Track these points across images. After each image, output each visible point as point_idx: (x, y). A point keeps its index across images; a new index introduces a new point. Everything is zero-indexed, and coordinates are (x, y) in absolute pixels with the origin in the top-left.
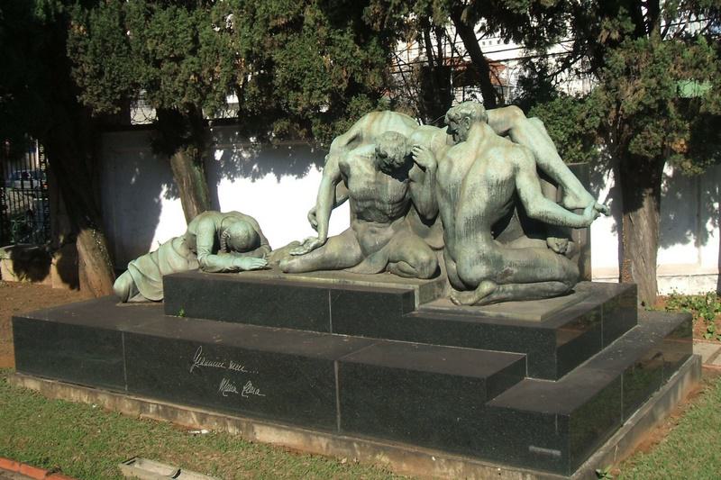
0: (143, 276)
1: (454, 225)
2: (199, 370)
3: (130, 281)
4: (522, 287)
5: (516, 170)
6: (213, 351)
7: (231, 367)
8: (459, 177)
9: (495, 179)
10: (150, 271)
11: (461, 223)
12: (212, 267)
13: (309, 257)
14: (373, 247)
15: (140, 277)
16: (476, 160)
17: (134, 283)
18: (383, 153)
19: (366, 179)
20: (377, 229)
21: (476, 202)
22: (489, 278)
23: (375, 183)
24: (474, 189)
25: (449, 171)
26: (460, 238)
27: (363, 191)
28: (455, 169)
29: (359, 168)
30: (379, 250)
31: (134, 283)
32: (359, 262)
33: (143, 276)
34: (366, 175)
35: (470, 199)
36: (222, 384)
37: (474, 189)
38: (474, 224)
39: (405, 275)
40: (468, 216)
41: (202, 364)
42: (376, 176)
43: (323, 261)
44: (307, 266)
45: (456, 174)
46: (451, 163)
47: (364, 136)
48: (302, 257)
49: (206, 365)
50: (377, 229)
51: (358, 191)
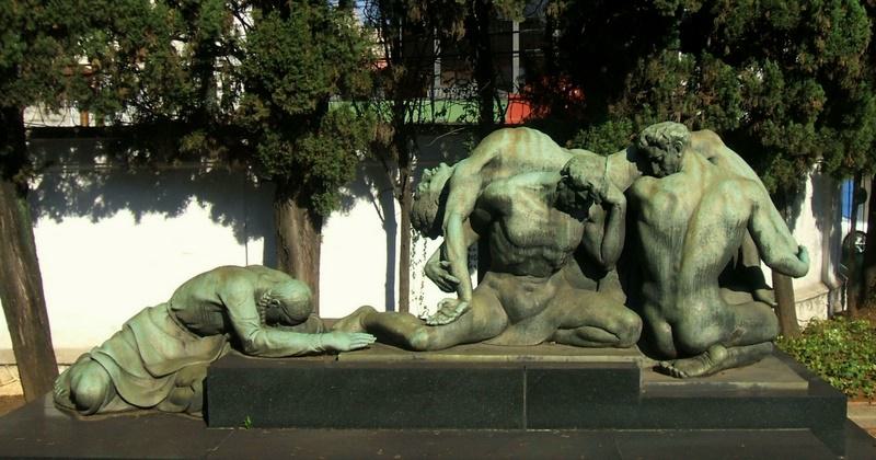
0: (121, 369)
1: (675, 278)
3: (106, 380)
4: (745, 350)
5: (754, 208)
8: (685, 217)
9: (736, 219)
10: (129, 361)
11: (690, 273)
12: (284, 349)
13: (453, 326)
14: (532, 310)
15: (118, 371)
16: (703, 194)
17: (111, 381)
19: (538, 218)
20: (533, 285)
21: (710, 249)
22: (721, 342)
23: (548, 224)
24: (708, 232)
25: (672, 209)
26: (686, 294)
27: (532, 235)
28: (680, 207)
29: (526, 204)
30: (539, 313)
31: (111, 381)
32: (505, 328)
33: (121, 369)
34: (537, 213)
35: (704, 243)
37: (708, 232)
38: (702, 278)
39: (593, 344)
40: (700, 265)
42: (550, 215)
43: (472, 331)
44: (451, 340)
45: (681, 213)
46: (673, 198)
47: (505, 159)
48: (447, 328)
50: (533, 285)
51: (526, 233)
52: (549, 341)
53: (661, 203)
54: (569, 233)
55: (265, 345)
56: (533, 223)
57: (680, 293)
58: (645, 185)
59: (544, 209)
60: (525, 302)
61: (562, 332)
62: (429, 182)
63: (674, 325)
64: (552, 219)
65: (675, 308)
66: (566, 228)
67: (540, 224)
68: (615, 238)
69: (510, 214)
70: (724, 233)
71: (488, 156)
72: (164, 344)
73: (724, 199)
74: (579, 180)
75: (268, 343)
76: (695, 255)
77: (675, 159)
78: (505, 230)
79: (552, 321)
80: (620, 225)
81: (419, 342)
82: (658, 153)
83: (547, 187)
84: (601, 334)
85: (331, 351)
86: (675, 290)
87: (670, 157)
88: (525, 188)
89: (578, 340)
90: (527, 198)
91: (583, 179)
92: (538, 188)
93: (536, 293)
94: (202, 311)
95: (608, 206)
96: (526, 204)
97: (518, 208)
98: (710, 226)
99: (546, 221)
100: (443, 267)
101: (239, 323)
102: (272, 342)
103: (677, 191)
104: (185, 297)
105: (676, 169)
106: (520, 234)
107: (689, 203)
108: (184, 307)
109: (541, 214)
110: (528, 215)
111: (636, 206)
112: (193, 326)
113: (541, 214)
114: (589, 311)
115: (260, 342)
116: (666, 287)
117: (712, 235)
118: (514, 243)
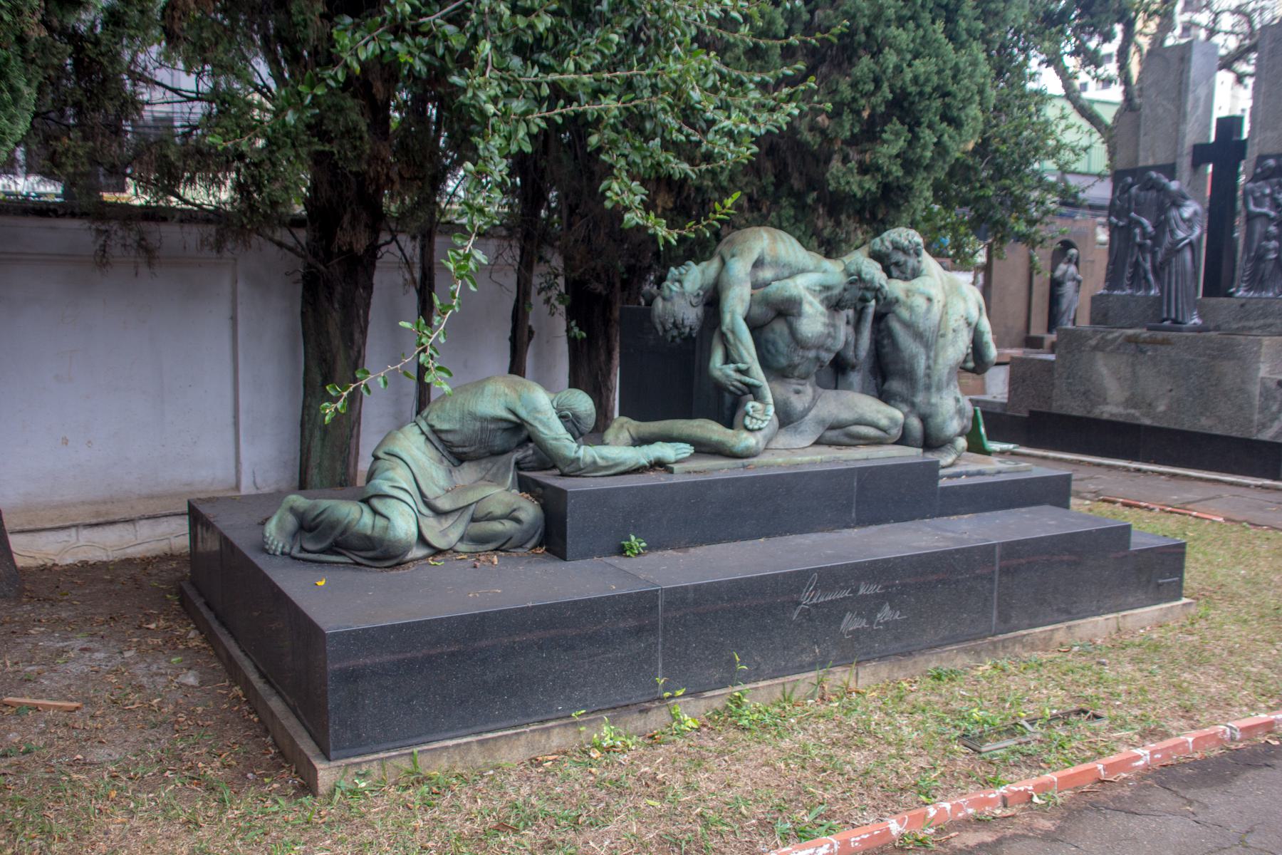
1: (928, 376)
2: (806, 614)
6: (830, 577)
7: (862, 591)
8: (938, 318)
12: (616, 465)
16: (946, 297)
20: (800, 387)
25: (928, 310)
26: (939, 389)
29: (811, 304)
35: (954, 342)
36: (845, 621)
41: (815, 601)
46: (929, 300)
47: (768, 259)
49: (822, 600)
50: (800, 387)
52: (818, 443)
53: (920, 302)
55: (595, 462)
57: (933, 390)
60: (798, 403)
61: (832, 435)
62: (680, 281)
63: (924, 419)
65: (929, 404)
69: (800, 314)
71: (755, 256)
72: (434, 474)
73: (965, 300)
74: (872, 281)
75: (598, 460)
78: (793, 332)
79: (821, 422)
81: (748, 448)
82: (900, 257)
83: (827, 288)
84: (871, 432)
85: (659, 465)
86: (928, 388)
87: (912, 262)
89: (846, 440)
91: (876, 280)
92: (818, 288)
93: (802, 396)
94: (482, 430)
96: (811, 304)
97: (807, 308)
100: (739, 371)
101: (556, 439)
102: (603, 458)
104: (457, 415)
105: (916, 273)
108: (457, 427)
110: (813, 320)
112: (455, 450)
114: (860, 411)
115: (588, 459)
116: (922, 381)
118: (798, 342)
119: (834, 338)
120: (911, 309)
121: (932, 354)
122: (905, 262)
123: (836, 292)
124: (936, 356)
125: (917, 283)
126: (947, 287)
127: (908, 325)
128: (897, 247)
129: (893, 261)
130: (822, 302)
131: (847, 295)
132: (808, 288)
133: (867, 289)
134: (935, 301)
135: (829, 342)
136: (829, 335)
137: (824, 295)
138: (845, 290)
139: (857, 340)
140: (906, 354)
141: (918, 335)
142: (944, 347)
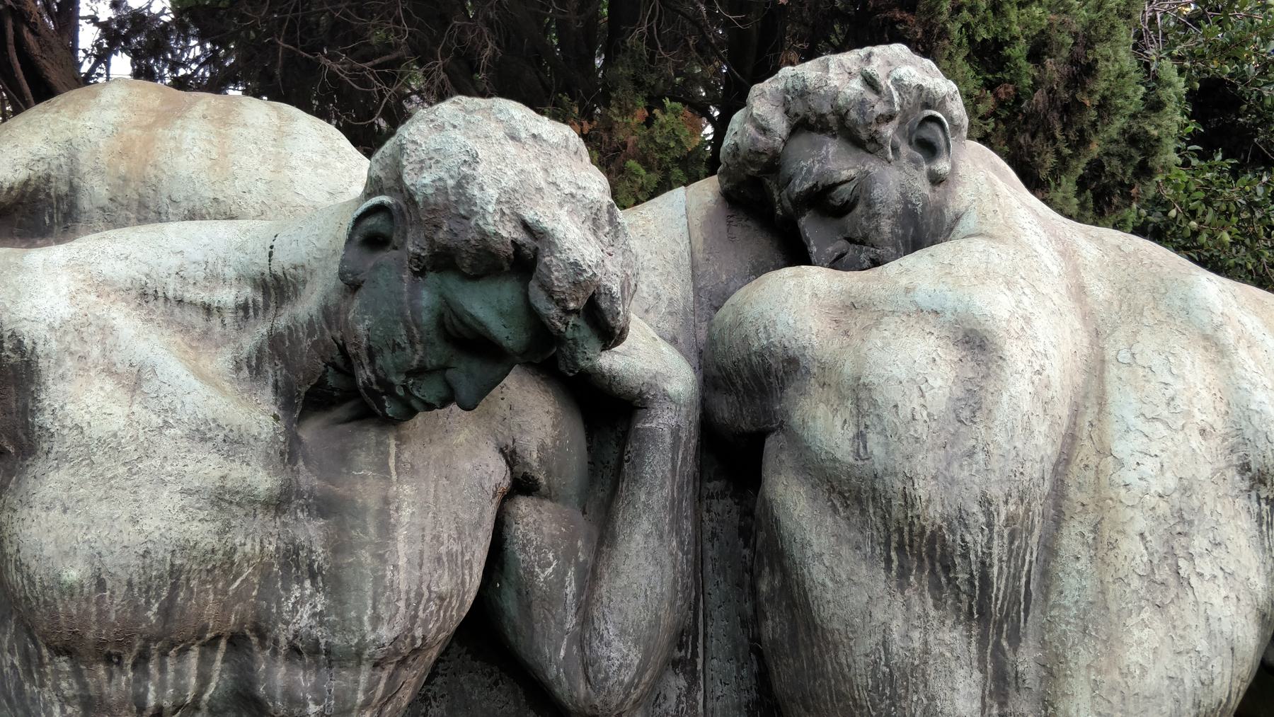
8: (1041, 446)
18: (509, 231)
19: (208, 468)
23: (279, 504)
24: (1180, 523)
25: (972, 404)
29: (135, 380)
34: (201, 435)
35: (1169, 579)
37: (1180, 523)
42: (291, 452)
46: (975, 342)
47: (96, 190)
53: (911, 366)
54: (402, 550)
56: (169, 499)
58: (795, 303)
59: (258, 415)
64: (308, 479)
66: (386, 528)
67: (223, 499)
68: (646, 568)
70: (1247, 523)
76: (1133, 657)
77: (922, 186)
80: (675, 506)
82: (831, 161)
83: (276, 287)
87: (894, 180)
88: (146, 295)
90: (140, 339)
91: (487, 195)
92: (227, 296)
95: (607, 412)
96: (135, 380)
98: (1186, 489)
99: (263, 481)
103: (995, 305)
105: (922, 229)
106: (73, 574)
107: (1055, 372)
109: (234, 443)
111: (744, 416)
113: (234, 443)
117: (1199, 543)
119: (333, 583)
120: (859, 397)
121: (1026, 660)
122: (864, 184)
123: (307, 306)
124: (1052, 671)
125: (916, 272)
126: (1100, 291)
127: (854, 492)
128: (810, 121)
129: (801, 185)
130: (253, 367)
131: (361, 323)
132: (146, 295)
133: (442, 261)
134: (1016, 353)
135: (301, 610)
136: (292, 561)
137: (260, 329)
138: (352, 285)
139: (590, 578)
140: (860, 655)
141: (920, 550)
142: (1099, 619)
